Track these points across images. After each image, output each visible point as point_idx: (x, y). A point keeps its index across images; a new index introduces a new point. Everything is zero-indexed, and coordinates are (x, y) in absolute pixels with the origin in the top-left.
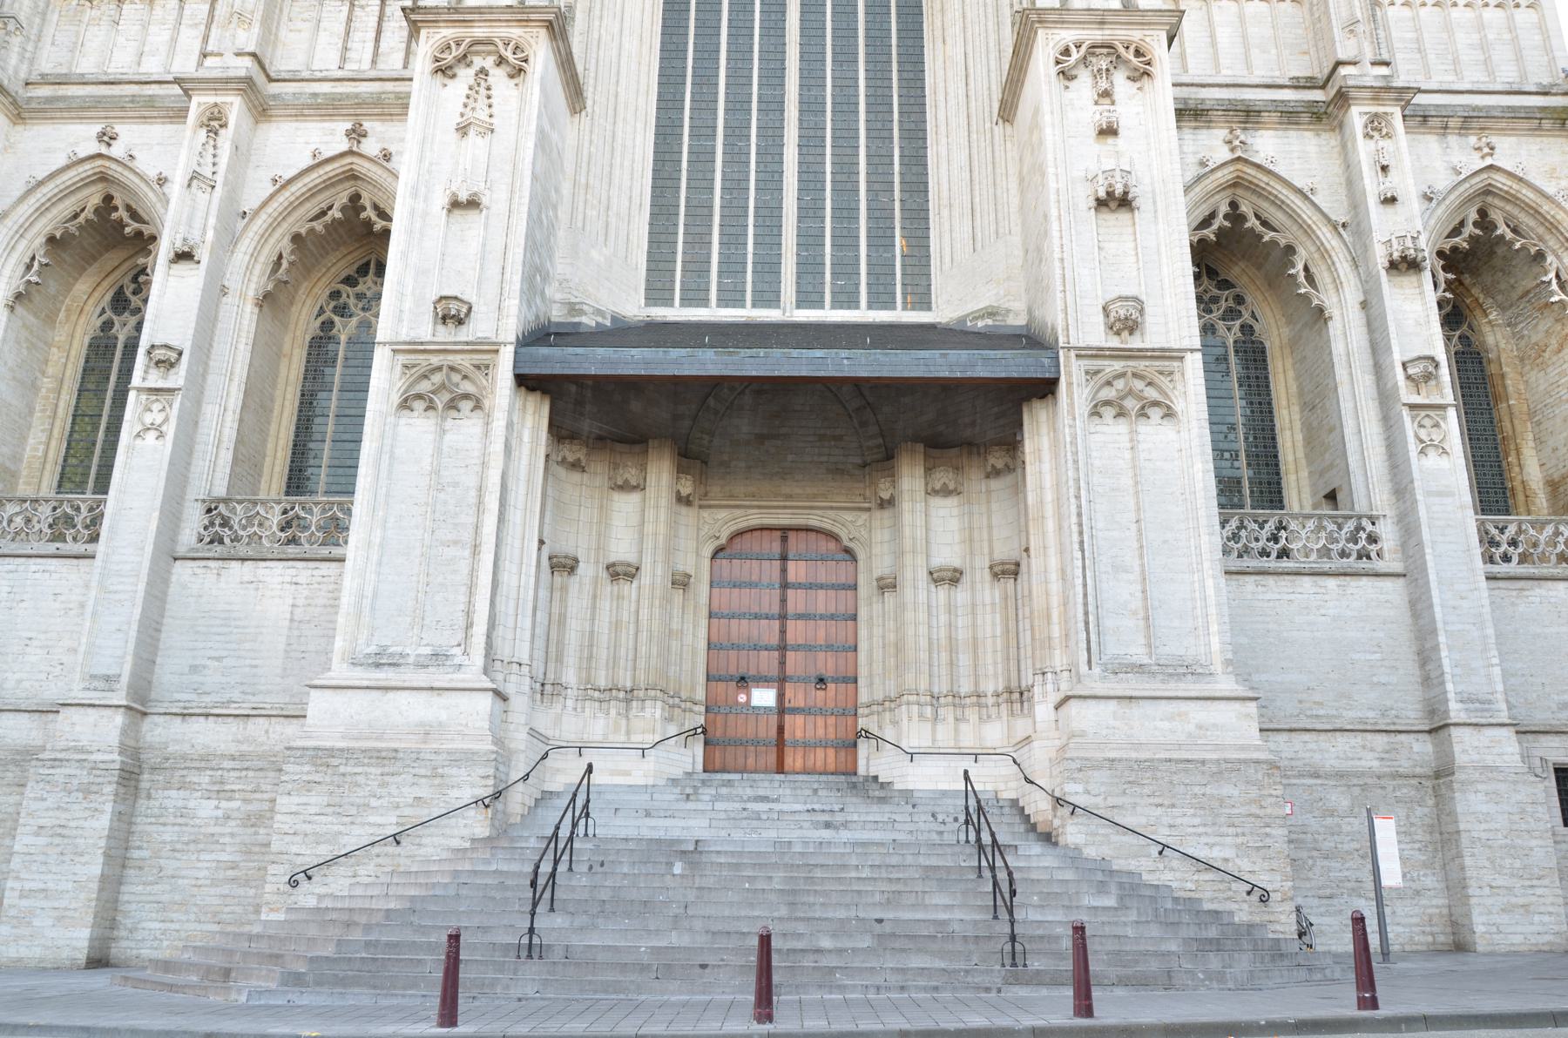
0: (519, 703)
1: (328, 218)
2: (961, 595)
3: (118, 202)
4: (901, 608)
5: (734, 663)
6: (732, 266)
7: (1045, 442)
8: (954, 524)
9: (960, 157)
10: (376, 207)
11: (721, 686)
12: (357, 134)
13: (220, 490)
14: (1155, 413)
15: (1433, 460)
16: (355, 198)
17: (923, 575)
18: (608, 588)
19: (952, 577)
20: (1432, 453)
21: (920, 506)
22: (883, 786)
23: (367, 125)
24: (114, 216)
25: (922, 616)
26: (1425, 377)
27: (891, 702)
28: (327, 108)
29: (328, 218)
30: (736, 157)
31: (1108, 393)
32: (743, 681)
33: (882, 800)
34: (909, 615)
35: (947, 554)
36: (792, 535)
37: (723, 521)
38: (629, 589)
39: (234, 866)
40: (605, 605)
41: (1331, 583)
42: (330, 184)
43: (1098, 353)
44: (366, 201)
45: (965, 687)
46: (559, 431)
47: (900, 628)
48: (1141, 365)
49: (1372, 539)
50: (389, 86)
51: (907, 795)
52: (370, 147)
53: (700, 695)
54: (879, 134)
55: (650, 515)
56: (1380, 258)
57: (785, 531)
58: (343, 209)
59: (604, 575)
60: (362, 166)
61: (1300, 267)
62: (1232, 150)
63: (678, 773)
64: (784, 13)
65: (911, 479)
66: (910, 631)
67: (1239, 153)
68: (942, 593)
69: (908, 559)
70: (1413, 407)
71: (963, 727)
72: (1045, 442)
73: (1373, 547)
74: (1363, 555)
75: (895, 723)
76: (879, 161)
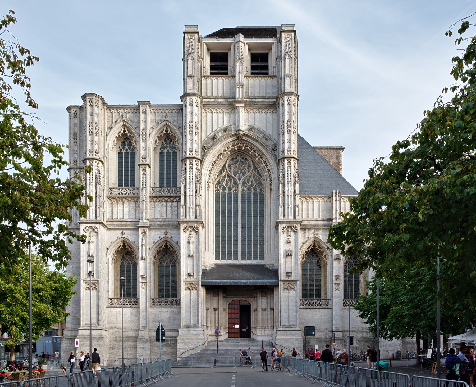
0: (205, 331)
1: (162, 248)
2: (266, 312)
3: (126, 244)
4: (257, 314)
5: (232, 321)
6: (230, 253)
7: (277, 293)
8: (265, 301)
9: (269, 233)
10: (170, 246)
11: (230, 325)
12: (166, 233)
13: (153, 298)
14: (292, 290)
15: (337, 292)
16: (166, 244)
17: (260, 309)
18: (213, 312)
19: (264, 310)
20: (337, 290)
21: (260, 299)
22: (255, 340)
23: (167, 231)
24: (126, 247)
25: (260, 316)
26: (337, 278)
27: (256, 328)
28: (160, 228)
29: (162, 248)
30: (230, 230)
31: (286, 287)
32: (234, 324)
33: (254, 342)
34: (258, 316)
35: (264, 306)
36: (241, 301)
37: (230, 299)
38: (217, 312)
39: (166, 352)
40: (213, 314)
41: (321, 310)
42: (163, 242)
43: (285, 281)
44: (168, 244)
45: (266, 326)
46: (207, 290)
47: (257, 317)
48: (291, 282)
49: (328, 303)
50: (170, 222)
51: (257, 341)
52: (169, 235)
53: (228, 326)
54: (255, 225)
55: (219, 301)
56: (334, 258)
57: (239, 300)
58: (165, 246)
59: (213, 310)
60: (168, 239)
61: (324, 255)
62: (314, 235)
63: (225, 338)
64: (238, 214)
65: (259, 296)
66: (258, 318)
67: (315, 236)
68: (263, 312)
69: (258, 307)
70: (335, 283)
71: (266, 332)
72: (277, 293)
73: (328, 304)
74: (327, 305)
75: (256, 331)
76: (255, 230)
